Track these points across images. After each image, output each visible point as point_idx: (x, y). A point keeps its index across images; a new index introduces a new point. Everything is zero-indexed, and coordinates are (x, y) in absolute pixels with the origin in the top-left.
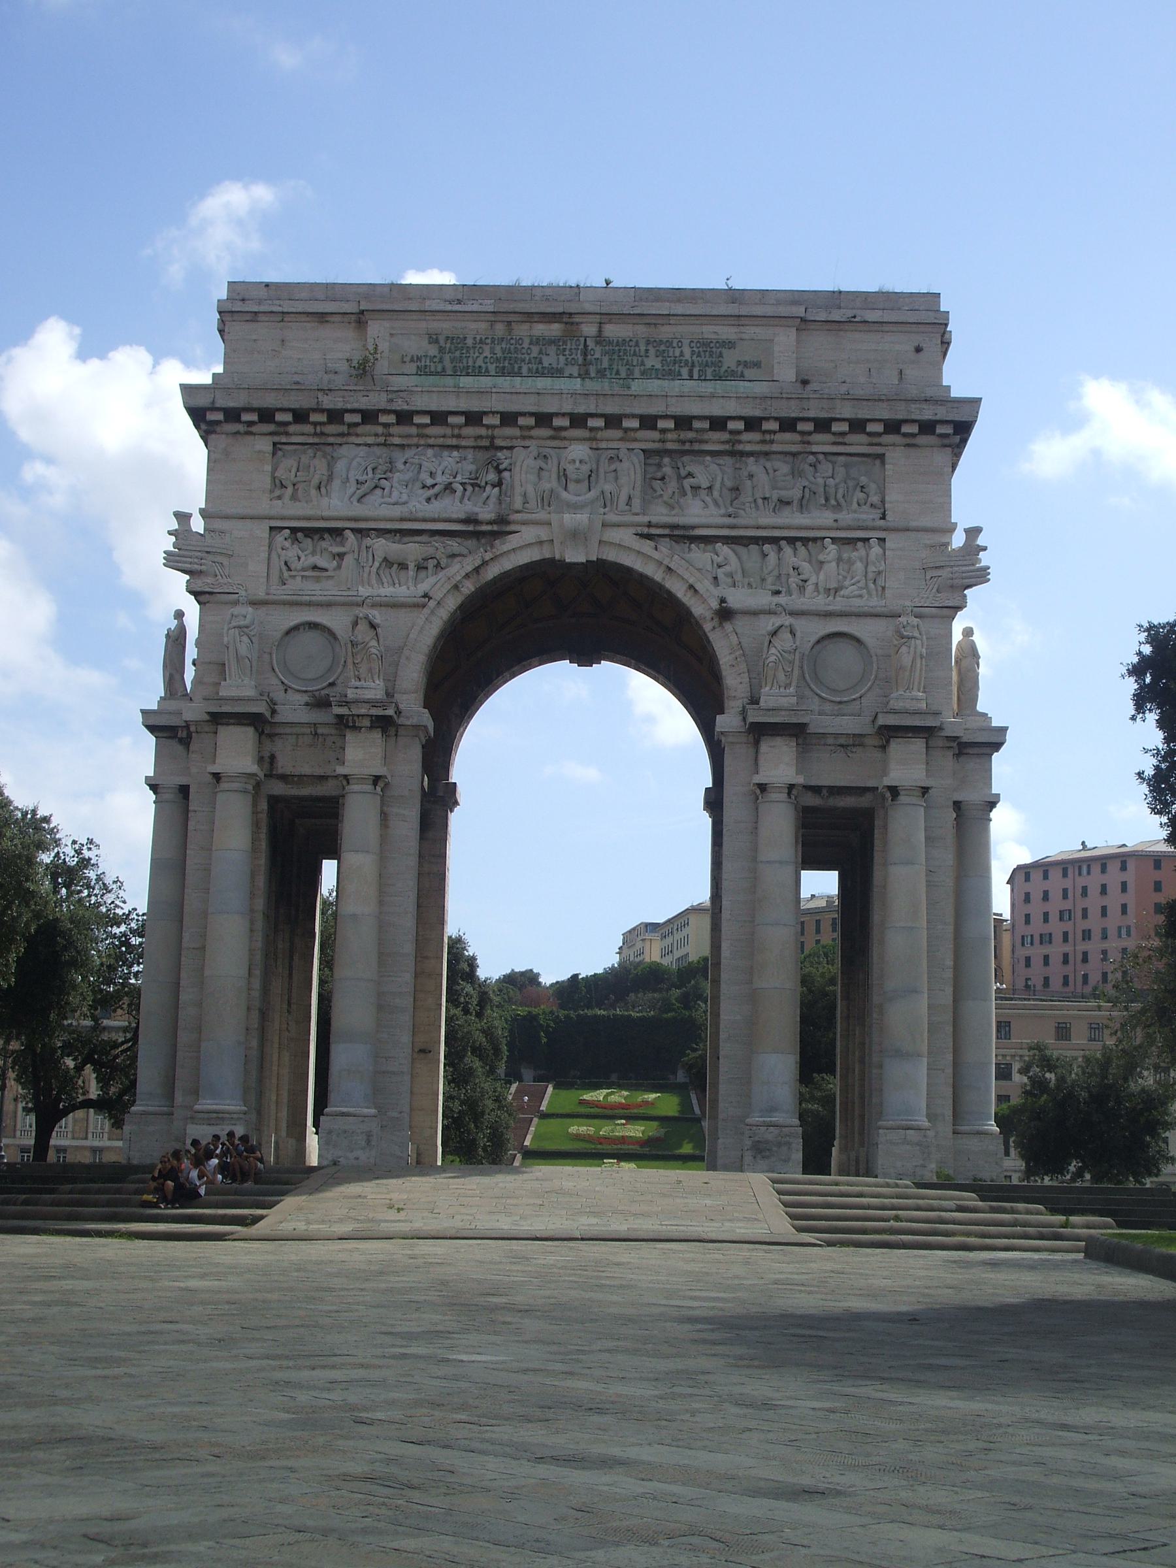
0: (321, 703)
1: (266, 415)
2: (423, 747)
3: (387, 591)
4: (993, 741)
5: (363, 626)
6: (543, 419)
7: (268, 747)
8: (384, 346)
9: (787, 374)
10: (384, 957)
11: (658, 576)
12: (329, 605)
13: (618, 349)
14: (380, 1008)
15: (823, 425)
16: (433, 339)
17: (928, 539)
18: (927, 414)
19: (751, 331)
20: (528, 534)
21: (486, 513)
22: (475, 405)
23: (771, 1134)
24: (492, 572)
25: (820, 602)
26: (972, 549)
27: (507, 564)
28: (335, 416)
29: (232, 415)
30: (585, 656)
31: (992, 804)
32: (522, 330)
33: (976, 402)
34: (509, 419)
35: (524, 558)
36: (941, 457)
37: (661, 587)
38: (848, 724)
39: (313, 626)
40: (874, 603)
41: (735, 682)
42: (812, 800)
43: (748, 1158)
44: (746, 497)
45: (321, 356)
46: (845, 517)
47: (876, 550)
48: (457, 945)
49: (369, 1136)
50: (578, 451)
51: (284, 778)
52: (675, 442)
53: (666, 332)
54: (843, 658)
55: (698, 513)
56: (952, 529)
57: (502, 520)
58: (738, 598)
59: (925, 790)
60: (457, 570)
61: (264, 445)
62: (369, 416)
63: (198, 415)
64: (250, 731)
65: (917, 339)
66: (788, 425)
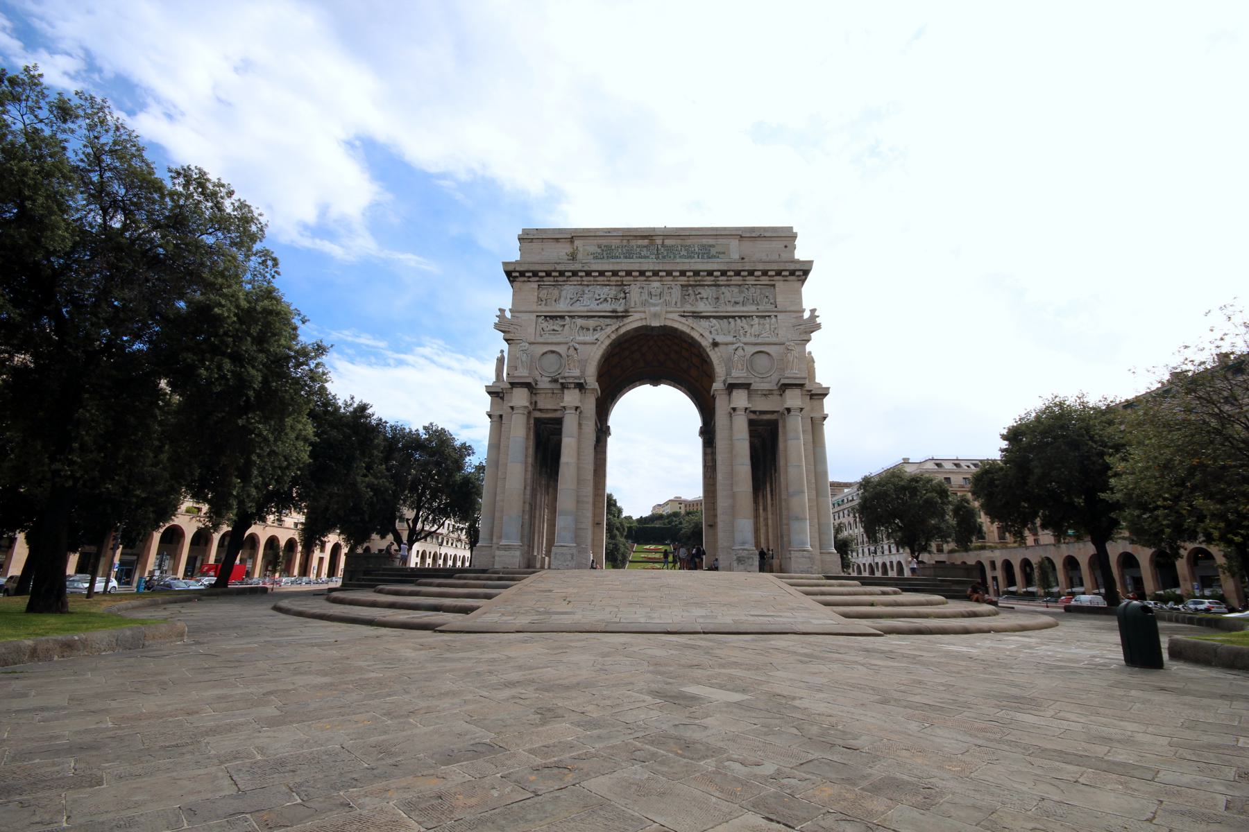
0: (555, 381)
1: (535, 274)
2: (597, 400)
3: (581, 338)
4: (823, 393)
5: (572, 349)
6: (642, 273)
7: (534, 398)
8: (581, 249)
9: (736, 256)
10: (579, 481)
11: (687, 330)
12: (559, 344)
13: (670, 249)
14: (578, 502)
15: (751, 273)
16: (599, 247)
17: (794, 315)
18: (792, 267)
19: (721, 241)
20: (637, 316)
21: (620, 309)
22: (616, 268)
23: (745, 553)
24: (623, 331)
25: (753, 340)
26: (813, 316)
27: (628, 328)
28: (562, 273)
29: (522, 274)
30: (655, 381)
31: (825, 418)
32: (633, 243)
33: (811, 262)
34: (629, 273)
35: (635, 325)
36: (797, 284)
37: (689, 335)
38: (766, 386)
39: (553, 352)
40: (774, 340)
41: (720, 370)
42: (753, 417)
43: (735, 564)
44: (722, 301)
45: (556, 255)
46: (761, 308)
47: (774, 319)
48: (610, 497)
49: (572, 555)
50: (656, 284)
51: (540, 410)
52: (694, 280)
53: (688, 242)
54: (762, 361)
55: (702, 307)
56: (803, 311)
57: (626, 311)
58: (719, 339)
59: (801, 409)
60: (609, 330)
61: (535, 285)
62: (575, 273)
63: (509, 274)
64: (526, 390)
65: (785, 243)
66: (738, 273)
